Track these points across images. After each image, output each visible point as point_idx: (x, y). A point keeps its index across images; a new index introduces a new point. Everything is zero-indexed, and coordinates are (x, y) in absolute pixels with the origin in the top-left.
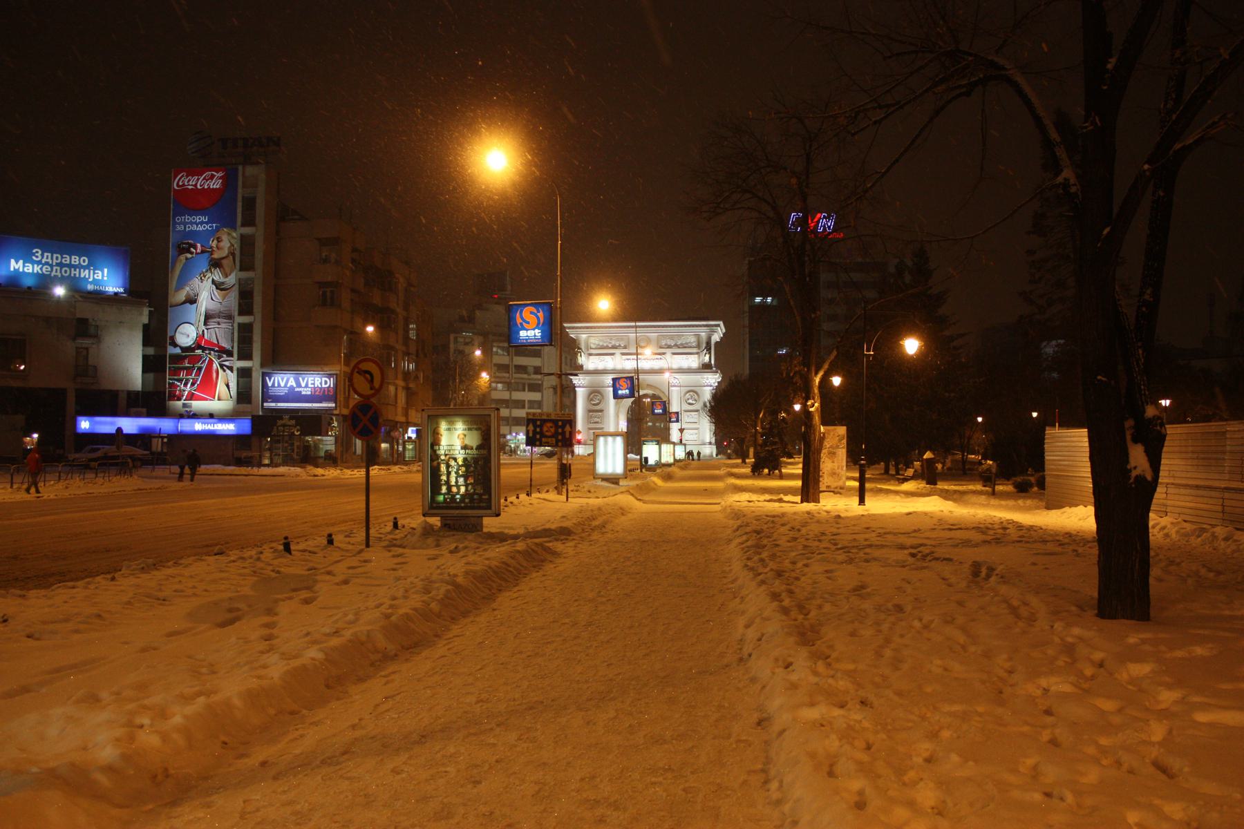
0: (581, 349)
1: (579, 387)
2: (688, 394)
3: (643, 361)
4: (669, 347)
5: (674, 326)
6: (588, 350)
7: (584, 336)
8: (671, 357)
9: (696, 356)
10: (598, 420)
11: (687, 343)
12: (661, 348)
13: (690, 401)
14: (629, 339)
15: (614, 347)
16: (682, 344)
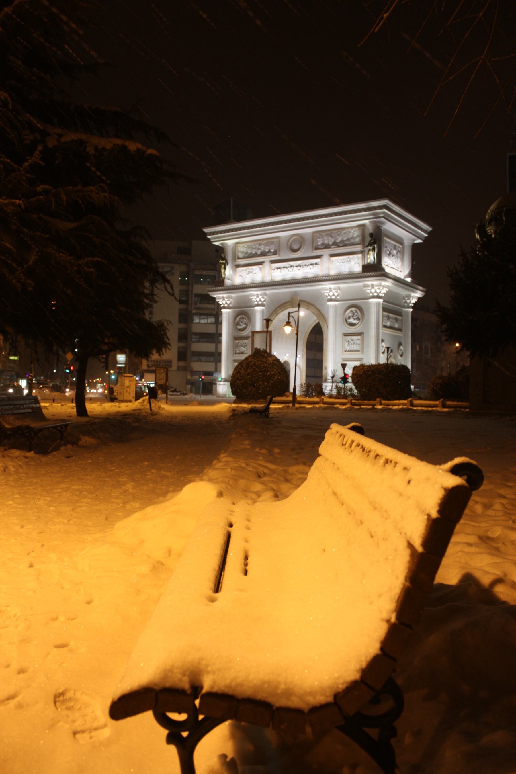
1: (224, 308)
2: (349, 311)
3: (295, 268)
4: (327, 246)
5: (326, 216)
6: (235, 261)
7: (230, 243)
8: (329, 259)
9: (360, 256)
10: (243, 349)
11: (348, 240)
12: (317, 248)
13: (351, 320)
14: (279, 242)
15: (264, 254)
16: (342, 241)
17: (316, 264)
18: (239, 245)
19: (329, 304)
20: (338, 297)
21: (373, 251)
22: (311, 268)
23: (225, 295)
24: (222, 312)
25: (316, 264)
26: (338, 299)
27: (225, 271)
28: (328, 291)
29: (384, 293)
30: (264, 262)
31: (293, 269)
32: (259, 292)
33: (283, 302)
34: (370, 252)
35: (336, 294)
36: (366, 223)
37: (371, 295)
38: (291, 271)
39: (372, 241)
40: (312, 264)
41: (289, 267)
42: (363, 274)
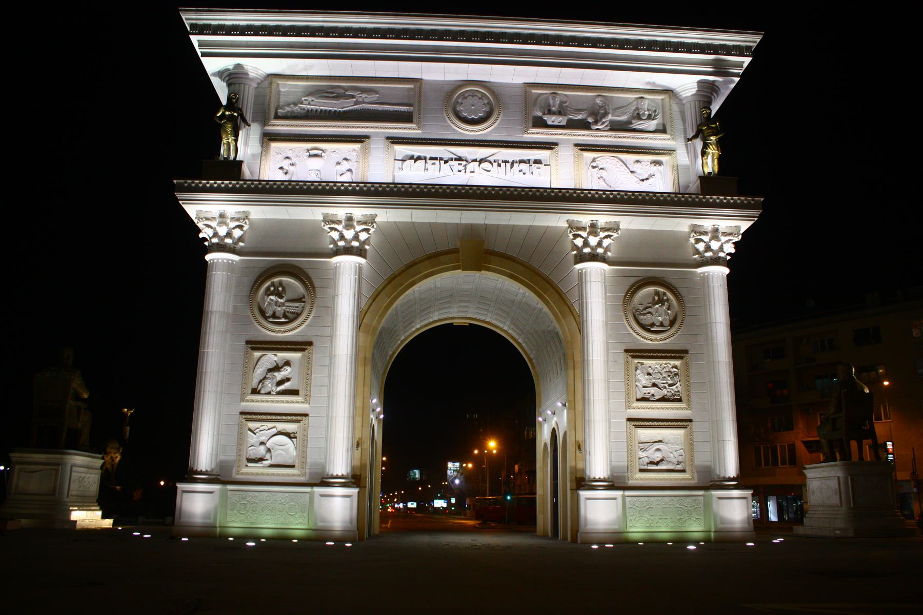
0: (239, 110)
8: (578, 157)
12: (540, 123)
14: (420, 93)
17: (537, 162)
18: (281, 82)
19: (579, 270)
20: (609, 254)
21: (718, 150)
22: (520, 171)
23: (232, 210)
24: (207, 262)
25: (537, 162)
26: (608, 257)
27: (236, 141)
28: (584, 234)
29: (728, 254)
30: (367, 137)
31: (465, 166)
32: (359, 213)
33: (432, 250)
34: (709, 150)
35: (606, 242)
36: (675, 89)
37: (709, 254)
38: (460, 171)
39: (713, 126)
40: (521, 161)
41: (452, 159)
42: (702, 196)
